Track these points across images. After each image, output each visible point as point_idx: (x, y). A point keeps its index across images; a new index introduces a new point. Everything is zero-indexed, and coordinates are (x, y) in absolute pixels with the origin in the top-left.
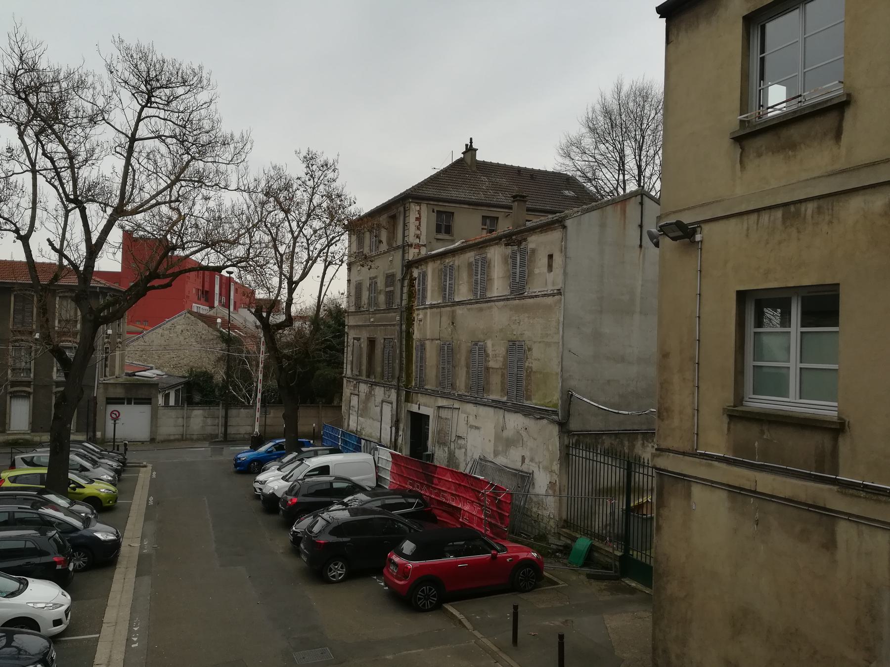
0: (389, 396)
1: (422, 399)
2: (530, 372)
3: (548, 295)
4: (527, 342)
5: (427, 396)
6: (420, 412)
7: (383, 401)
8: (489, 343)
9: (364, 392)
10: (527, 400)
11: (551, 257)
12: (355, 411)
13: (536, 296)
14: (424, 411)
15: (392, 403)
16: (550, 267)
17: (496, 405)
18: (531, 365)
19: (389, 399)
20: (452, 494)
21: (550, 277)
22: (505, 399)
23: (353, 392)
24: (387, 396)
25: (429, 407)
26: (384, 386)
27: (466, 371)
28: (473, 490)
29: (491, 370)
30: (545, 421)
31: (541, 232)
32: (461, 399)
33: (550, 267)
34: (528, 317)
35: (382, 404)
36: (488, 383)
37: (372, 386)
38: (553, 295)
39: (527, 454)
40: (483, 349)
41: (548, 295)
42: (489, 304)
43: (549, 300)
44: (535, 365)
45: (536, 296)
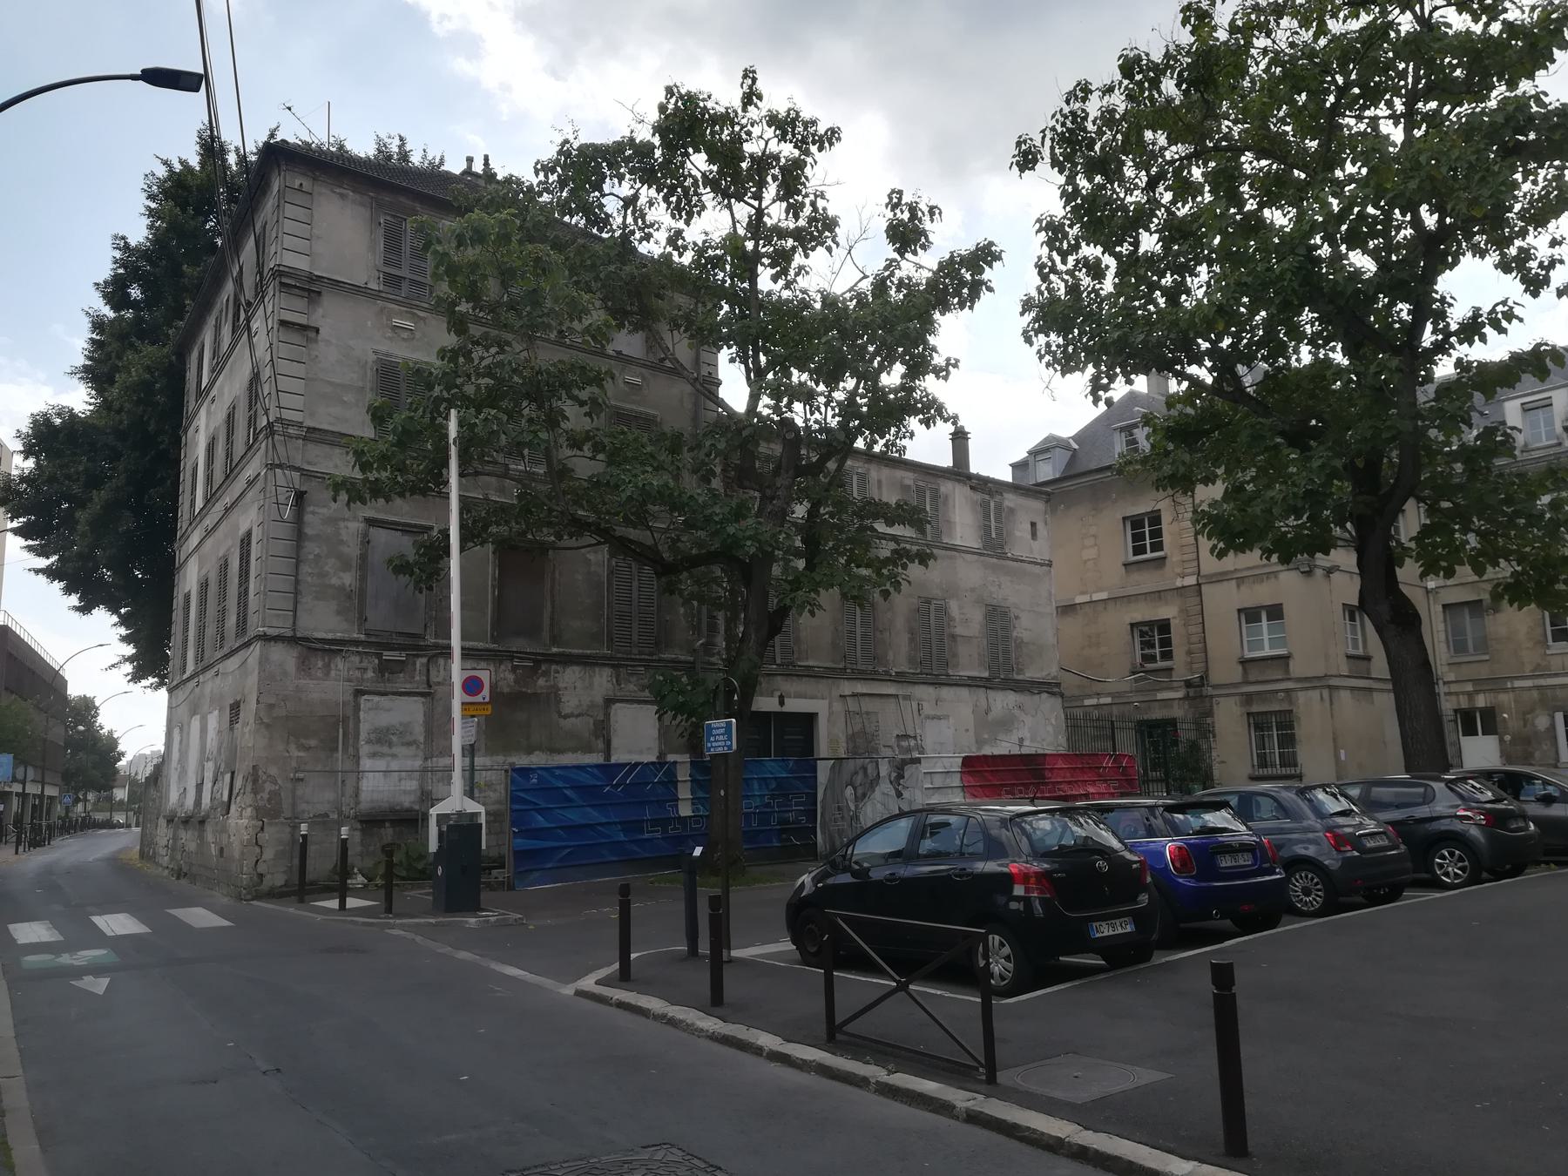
2: (1020, 644)
3: (1036, 563)
4: (1013, 610)
5: (804, 679)
6: (787, 709)
8: (954, 607)
10: (1018, 674)
11: (1033, 525)
13: (1022, 561)
16: (1034, 535)
17: (972, 683)
18: (1020, 635)
20: (1069, 783)
21: (1035, 545)
22: (986, 674)
26: (613, 666)
27: (909, 639)
28: (1090, 768)
29: (959, 639)
30: (1044, 696)
31: (1022, 495)
32: (901, 679)
33: (1034, 535)
34: (1011, 581)
36: (955, 655)
38: (1042, 565)
39: (1025, 733)
40: (943, 611)
41: (1036, 563)
42: (949, 553)
43: (1037, 569)
44: (1026, 636)
45: (1022, 561)
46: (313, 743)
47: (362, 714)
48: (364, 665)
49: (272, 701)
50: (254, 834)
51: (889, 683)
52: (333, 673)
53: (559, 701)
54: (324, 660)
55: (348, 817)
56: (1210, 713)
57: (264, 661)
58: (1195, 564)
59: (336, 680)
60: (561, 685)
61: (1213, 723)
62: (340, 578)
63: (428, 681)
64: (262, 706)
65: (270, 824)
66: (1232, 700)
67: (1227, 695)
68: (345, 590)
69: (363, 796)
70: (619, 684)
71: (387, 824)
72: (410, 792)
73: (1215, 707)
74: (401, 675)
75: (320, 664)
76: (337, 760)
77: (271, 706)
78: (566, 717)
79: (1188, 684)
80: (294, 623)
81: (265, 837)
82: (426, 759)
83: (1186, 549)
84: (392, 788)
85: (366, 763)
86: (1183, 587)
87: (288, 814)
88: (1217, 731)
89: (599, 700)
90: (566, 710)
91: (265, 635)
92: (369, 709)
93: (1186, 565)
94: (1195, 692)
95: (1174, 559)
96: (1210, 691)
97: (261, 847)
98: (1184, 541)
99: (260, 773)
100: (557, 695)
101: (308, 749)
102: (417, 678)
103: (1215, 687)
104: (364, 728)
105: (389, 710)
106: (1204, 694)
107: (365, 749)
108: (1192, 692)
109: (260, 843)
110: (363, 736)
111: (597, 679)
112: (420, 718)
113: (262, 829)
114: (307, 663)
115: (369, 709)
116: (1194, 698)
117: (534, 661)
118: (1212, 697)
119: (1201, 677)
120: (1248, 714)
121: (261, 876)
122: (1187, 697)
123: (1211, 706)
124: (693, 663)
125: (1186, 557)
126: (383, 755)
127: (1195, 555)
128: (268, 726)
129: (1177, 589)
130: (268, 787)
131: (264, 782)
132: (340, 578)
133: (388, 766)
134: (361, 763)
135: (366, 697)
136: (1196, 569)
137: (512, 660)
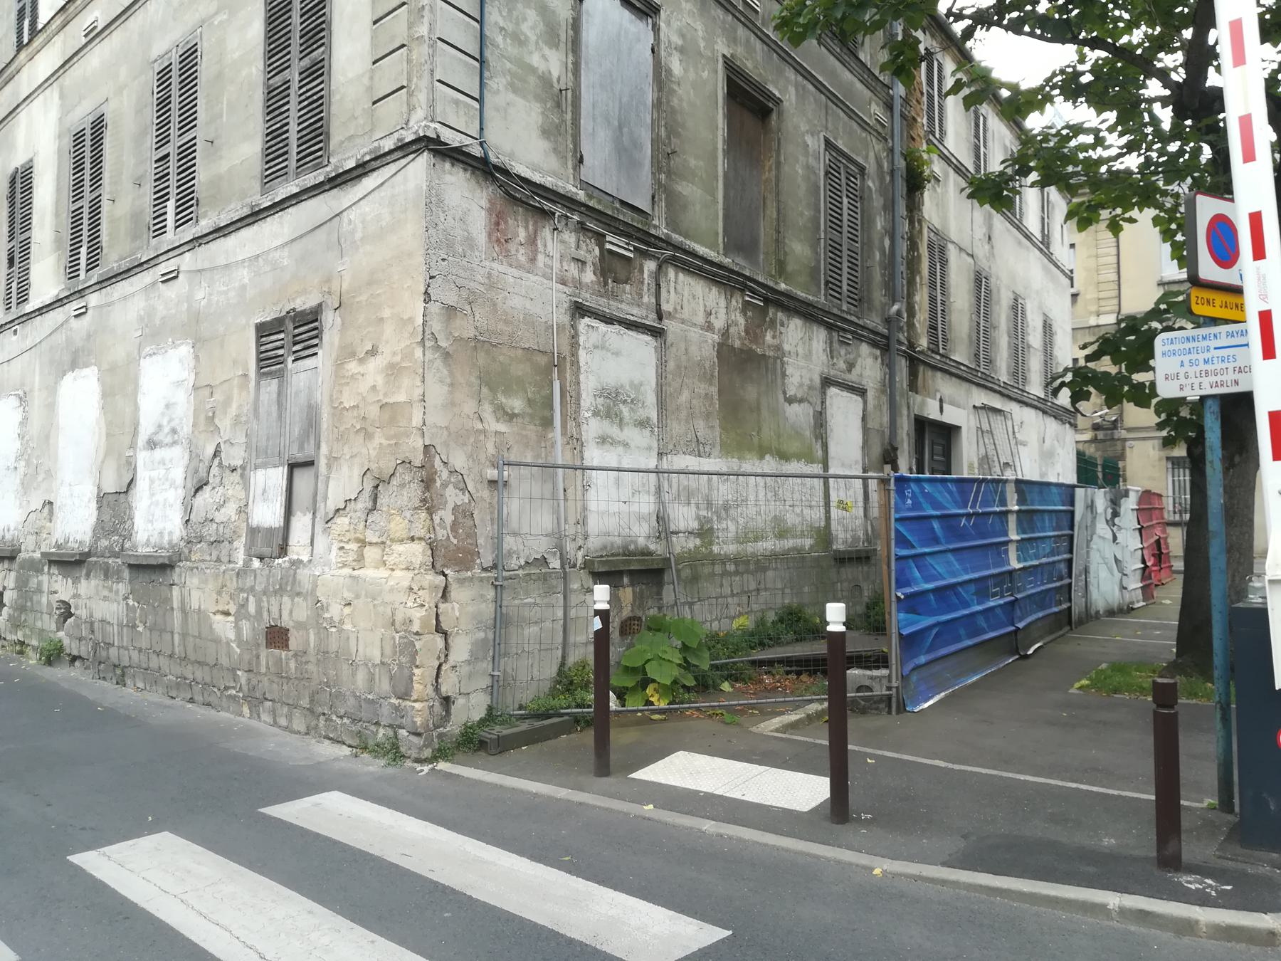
0: (851, 366)
1: (946, 386)
7: (827, 382)
9: (709, 327)
12: (643, 424)
13: (1058, 267)
14: (951, 416)
15: (861, 392)
19: (853, 377)
22: (1043, 396)
23: (588, 299)
24: (842, 365)
25: (958, 406)
35: (824, 393)
37: (764, 312)
45: (1058, 267)
46: (517, 404)
47: (582, 353)
48: (582, 253)
49: (452, 299)
50: (433, 605)
51: (998, 396)
52: (541, 258)
53: (784, 375)
54: (526, 228)
55: (574, 566)
56: (1122, 457)
57: (433, 201)
58: (1115, 301)
59: (544, 276)
60: (786, 347)
61: (1124, 467)
62: (544, 57)
63: (658, 305)
64: (434, 308)
65: (461, 581)
66: (1150, 443)
67: (1144, 439)
68: (552, 86)
69: (593, 525)
70: (832, 357)
71: (626, 580)
72: (640, 518)
73: (1128, 450)
74: (628, 287)
75: (522, 234)
76: (553, 445)
77: (450, 311)
78: (790, 401)
79: (1096, 427)
80: (481, 129)
81: (451, 611)
82: (660, 455)
83: (1102, 287)
84: (615, 507)
85: (594, 455)
86: (1098, 326)
87: (487, 558)
88: (1128, 474)
89: (817, 381)
90: (791, 392)
91: (437, 141)
92: (596, 347)
93: (1103, 303)
94: (1105, 435)
95: (1088, 297)
96: (1124, 434)
97: (445, 634)
98: (1102, 278)
99: (437, 463)
100: (783, 363)
101: (511, 417)
102: (646, 299)
103: (1129, 430)
104: (588, 385)
105: (617, 354)
106: (1116, 437)
107: (592, 428)
108: (1101, 435)
109: (444, 626)
110: (587, 401)
111: (815, 343)
112: (649, 376)
113: (445, 595)
114: (502, 226)
115: (596, 347)
116: (1103, 441)
117: (766, 300)
118: (1125, 440)
119: (1116, 421)
120: (1168, 458)
121: (447, 701)
122: (1094, 440)
123: (1124, 449)
124: (887, 338)
125: (1102, 295)
126: (614, 443)
127: (1115, 293)
128: (447, 355)
129: (1090, 327)
130: (453, 497)
131: (444, 485)
132: (544, 57)
133: (620, 462)
134: (586, 455)
135: (587, 320)
136: (1117, 308)
137: (743, 294)
